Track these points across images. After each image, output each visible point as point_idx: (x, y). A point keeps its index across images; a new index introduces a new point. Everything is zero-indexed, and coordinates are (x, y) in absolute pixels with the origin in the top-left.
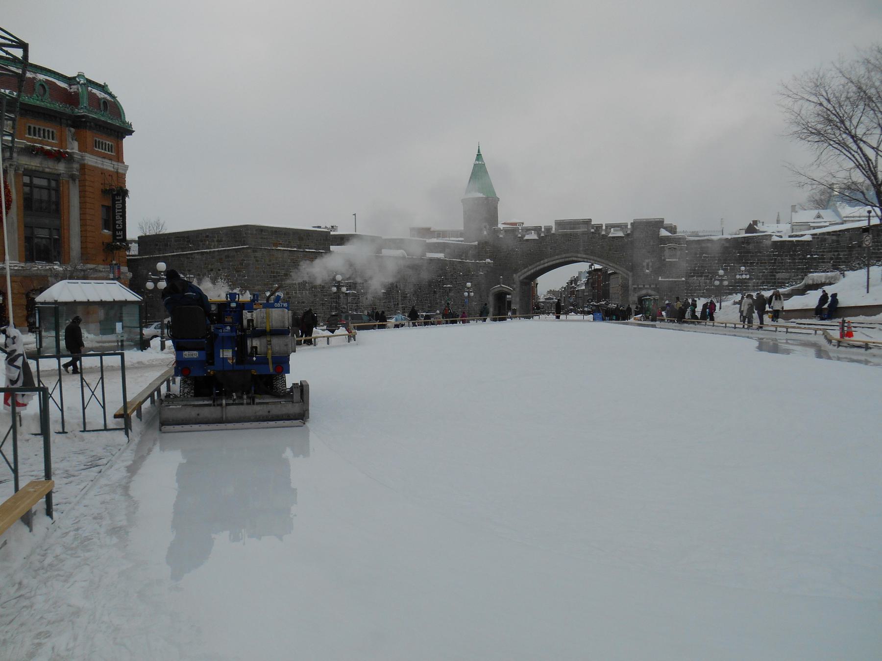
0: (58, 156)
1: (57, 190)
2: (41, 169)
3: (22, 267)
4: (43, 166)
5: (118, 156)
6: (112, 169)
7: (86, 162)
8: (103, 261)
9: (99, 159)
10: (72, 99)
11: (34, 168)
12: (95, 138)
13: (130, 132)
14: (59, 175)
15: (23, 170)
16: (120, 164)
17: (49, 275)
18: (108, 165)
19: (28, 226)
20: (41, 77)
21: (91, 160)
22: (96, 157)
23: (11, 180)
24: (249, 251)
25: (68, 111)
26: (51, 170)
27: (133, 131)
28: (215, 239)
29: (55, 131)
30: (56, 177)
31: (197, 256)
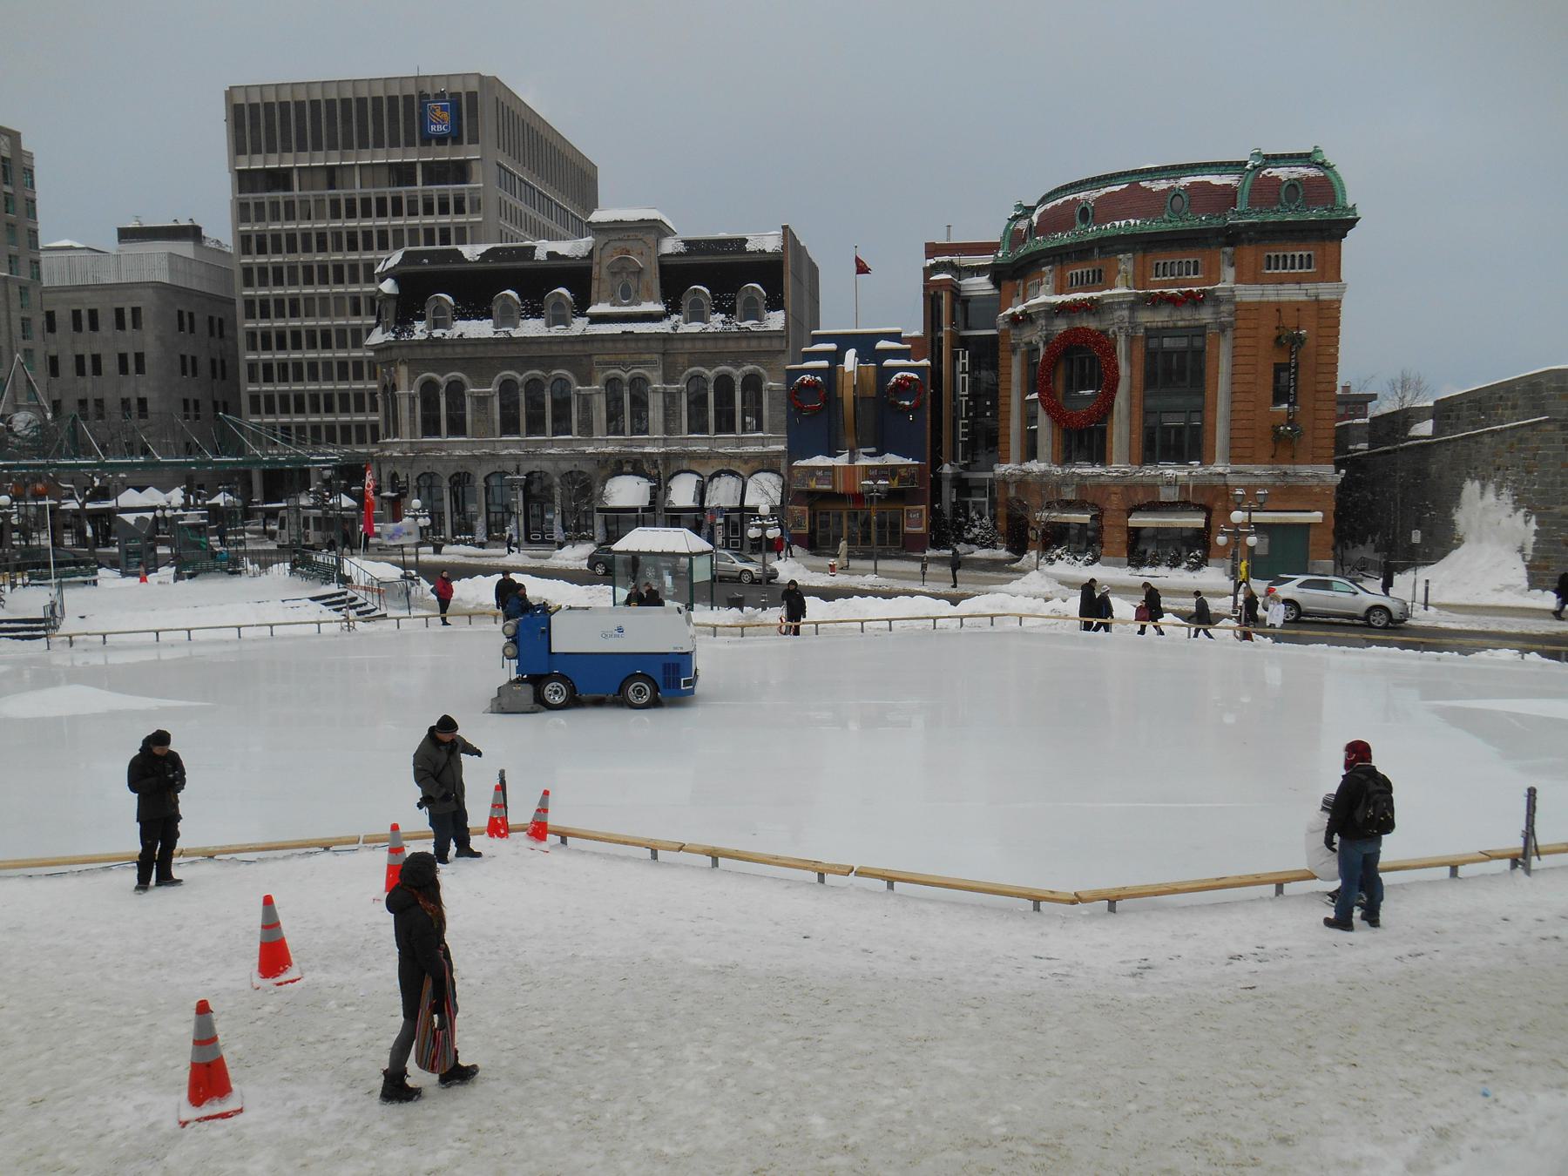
0: (1193, 300)
1: (1199, 354)
2: (1171, 324)
3: (1125, 473)
4: (1175, 318)
5: (1331, 271)
6: (1305, 298)
7: (1238, 299)
8: (1273, 457)
9: (1270, 287)
10: (1266, 191)
11: (1160, 324)
12: (1267, 254)
13: (1352, 223)
14: (1205, 326)
15: (1142, 331)
16: (1322, 285)
17: (1159, 483)
18: (1292, 293)
19: (1147, 412)
20: (1185, 181)
21: (1249, 293)
22: (1258, 287)
23: (1121, 349)
24: (1550, 427)
25: (1216, 223)
26: (1187, 323)
27: (1358, 219)
28: (1509, 403)
29: (1199, 260)
30: (1200, 331)
31: (1487, 439)
